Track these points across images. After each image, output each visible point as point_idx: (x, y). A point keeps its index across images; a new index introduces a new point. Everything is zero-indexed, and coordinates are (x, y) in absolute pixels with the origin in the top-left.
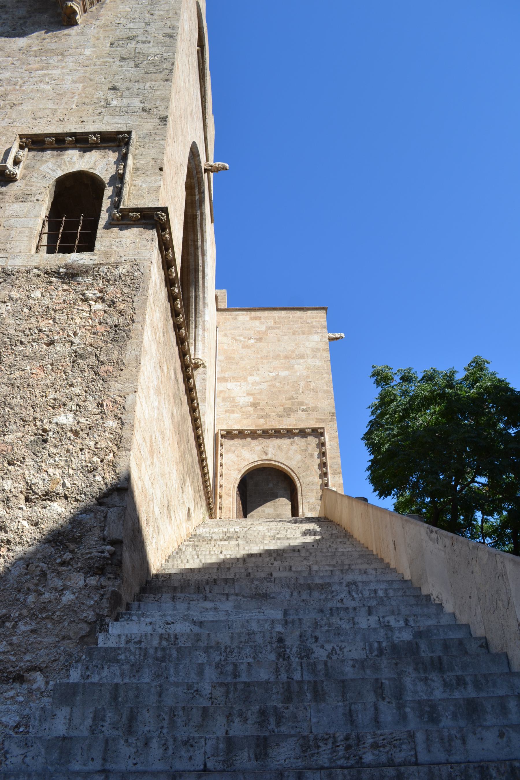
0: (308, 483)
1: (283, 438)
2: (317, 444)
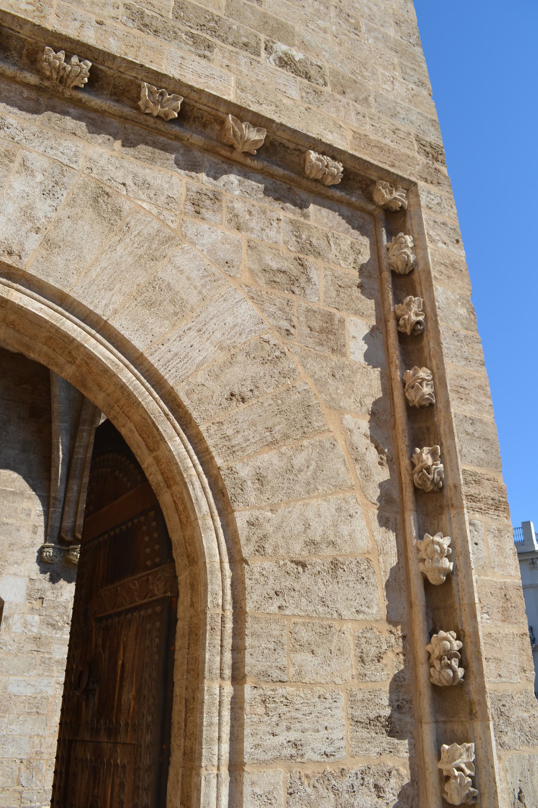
0: (298, 549)
1: (144, 150)
2: (362, 270)
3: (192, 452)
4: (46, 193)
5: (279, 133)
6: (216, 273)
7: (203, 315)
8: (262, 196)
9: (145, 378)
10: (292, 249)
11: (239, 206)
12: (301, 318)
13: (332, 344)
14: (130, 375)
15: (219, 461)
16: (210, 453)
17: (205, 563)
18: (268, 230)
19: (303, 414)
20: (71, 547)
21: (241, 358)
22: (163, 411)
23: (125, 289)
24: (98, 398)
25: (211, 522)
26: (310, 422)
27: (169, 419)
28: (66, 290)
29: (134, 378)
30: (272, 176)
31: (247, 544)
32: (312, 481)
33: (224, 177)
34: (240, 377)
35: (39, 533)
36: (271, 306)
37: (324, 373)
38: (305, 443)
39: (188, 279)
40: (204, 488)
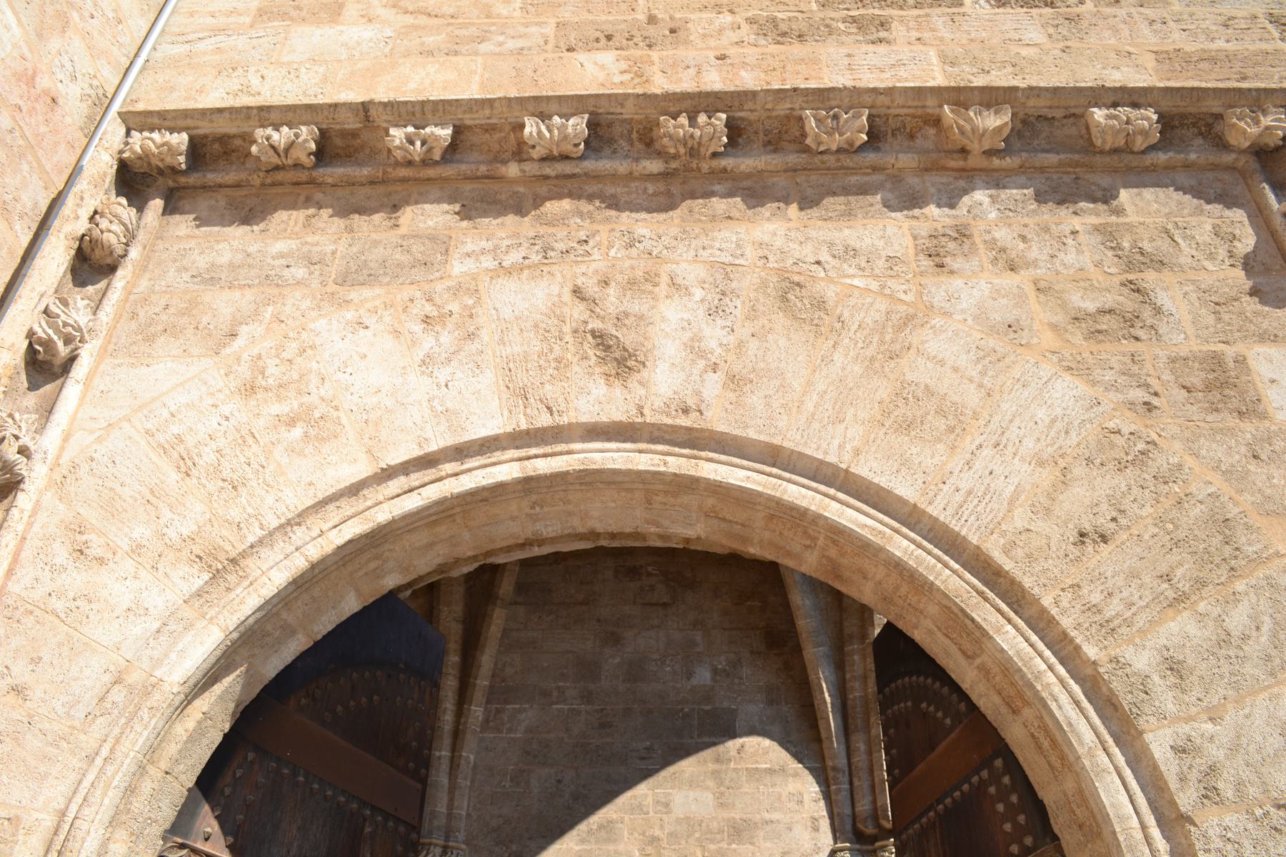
1: (834, 204)
2: (1249, 264)
3: (1041, 646)
4: (714, 312)
5: (1031, 103)
6: (997, 348)
7: (996, 418)
8: (1034, 206)
9: (930, 542)
10: (1112, 270)
11: (1003, 235)
12: (1164, 377)
13: (1234, 403)
14: (906, 543)
15: (1091, 651)
16: (1072, 640)
17: (1114, 833)
18: (1061, 255)
19: (1221, 538)
20: (878, 844)
21: (1079, 470)
22: (973, 587)
23: (861, 415)
24: (865, 594)
25: (1106, 759)
26: (1237, 549)
27: (986, 599)
28: (777, 441)
29: (913, 547)
30: (1042, 170)
31: (1182, 789)
32: (1274, 653)
33: (966, 199)
34: (1087, 501)
35: (822, 829)
36: (1105, 372)
37: (1237, 457)
38: (1240, 586)
39: (956, 370)
40: (1077, 703)
